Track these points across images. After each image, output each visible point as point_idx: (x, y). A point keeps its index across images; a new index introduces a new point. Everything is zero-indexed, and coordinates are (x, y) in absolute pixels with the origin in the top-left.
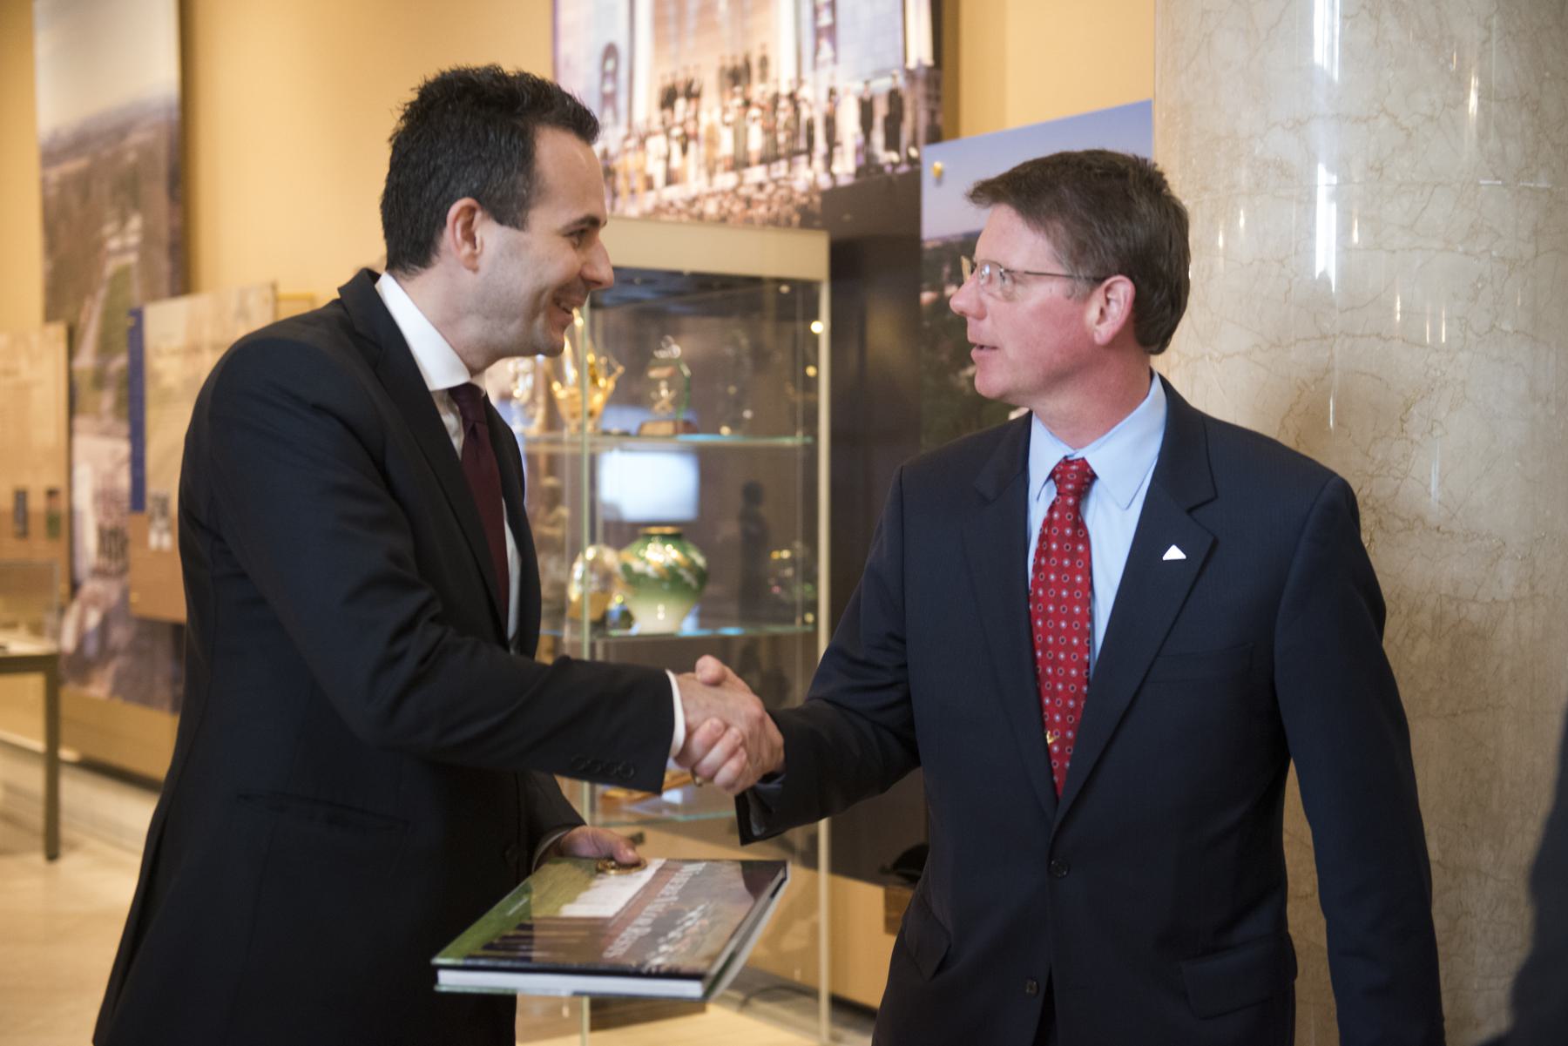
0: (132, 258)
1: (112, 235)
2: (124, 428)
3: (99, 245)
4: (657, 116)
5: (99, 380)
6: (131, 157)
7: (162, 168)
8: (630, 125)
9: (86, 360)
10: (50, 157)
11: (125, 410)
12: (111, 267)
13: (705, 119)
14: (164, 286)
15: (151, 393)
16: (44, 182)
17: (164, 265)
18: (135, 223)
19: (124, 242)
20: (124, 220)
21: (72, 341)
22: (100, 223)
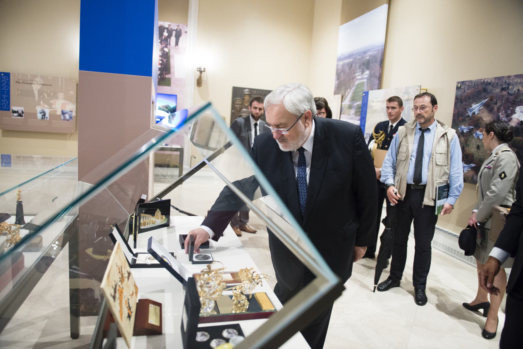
0: (366, 80)
1: (358, 76)
2: (359, 118)
3: (354, 78)
5: (350, 107)
6: (368, 58)
7: (379, 60)
9: (347, 102)
10: (340, 59)
11: (359, 114)
12: (357, 83)
14: (376, 87)
15: (369, 110)
16: (337, 65)
17: (377, 82)
18: (367, 72)
19: (362, 77)
20: (363, 72)
22: (355, 73)
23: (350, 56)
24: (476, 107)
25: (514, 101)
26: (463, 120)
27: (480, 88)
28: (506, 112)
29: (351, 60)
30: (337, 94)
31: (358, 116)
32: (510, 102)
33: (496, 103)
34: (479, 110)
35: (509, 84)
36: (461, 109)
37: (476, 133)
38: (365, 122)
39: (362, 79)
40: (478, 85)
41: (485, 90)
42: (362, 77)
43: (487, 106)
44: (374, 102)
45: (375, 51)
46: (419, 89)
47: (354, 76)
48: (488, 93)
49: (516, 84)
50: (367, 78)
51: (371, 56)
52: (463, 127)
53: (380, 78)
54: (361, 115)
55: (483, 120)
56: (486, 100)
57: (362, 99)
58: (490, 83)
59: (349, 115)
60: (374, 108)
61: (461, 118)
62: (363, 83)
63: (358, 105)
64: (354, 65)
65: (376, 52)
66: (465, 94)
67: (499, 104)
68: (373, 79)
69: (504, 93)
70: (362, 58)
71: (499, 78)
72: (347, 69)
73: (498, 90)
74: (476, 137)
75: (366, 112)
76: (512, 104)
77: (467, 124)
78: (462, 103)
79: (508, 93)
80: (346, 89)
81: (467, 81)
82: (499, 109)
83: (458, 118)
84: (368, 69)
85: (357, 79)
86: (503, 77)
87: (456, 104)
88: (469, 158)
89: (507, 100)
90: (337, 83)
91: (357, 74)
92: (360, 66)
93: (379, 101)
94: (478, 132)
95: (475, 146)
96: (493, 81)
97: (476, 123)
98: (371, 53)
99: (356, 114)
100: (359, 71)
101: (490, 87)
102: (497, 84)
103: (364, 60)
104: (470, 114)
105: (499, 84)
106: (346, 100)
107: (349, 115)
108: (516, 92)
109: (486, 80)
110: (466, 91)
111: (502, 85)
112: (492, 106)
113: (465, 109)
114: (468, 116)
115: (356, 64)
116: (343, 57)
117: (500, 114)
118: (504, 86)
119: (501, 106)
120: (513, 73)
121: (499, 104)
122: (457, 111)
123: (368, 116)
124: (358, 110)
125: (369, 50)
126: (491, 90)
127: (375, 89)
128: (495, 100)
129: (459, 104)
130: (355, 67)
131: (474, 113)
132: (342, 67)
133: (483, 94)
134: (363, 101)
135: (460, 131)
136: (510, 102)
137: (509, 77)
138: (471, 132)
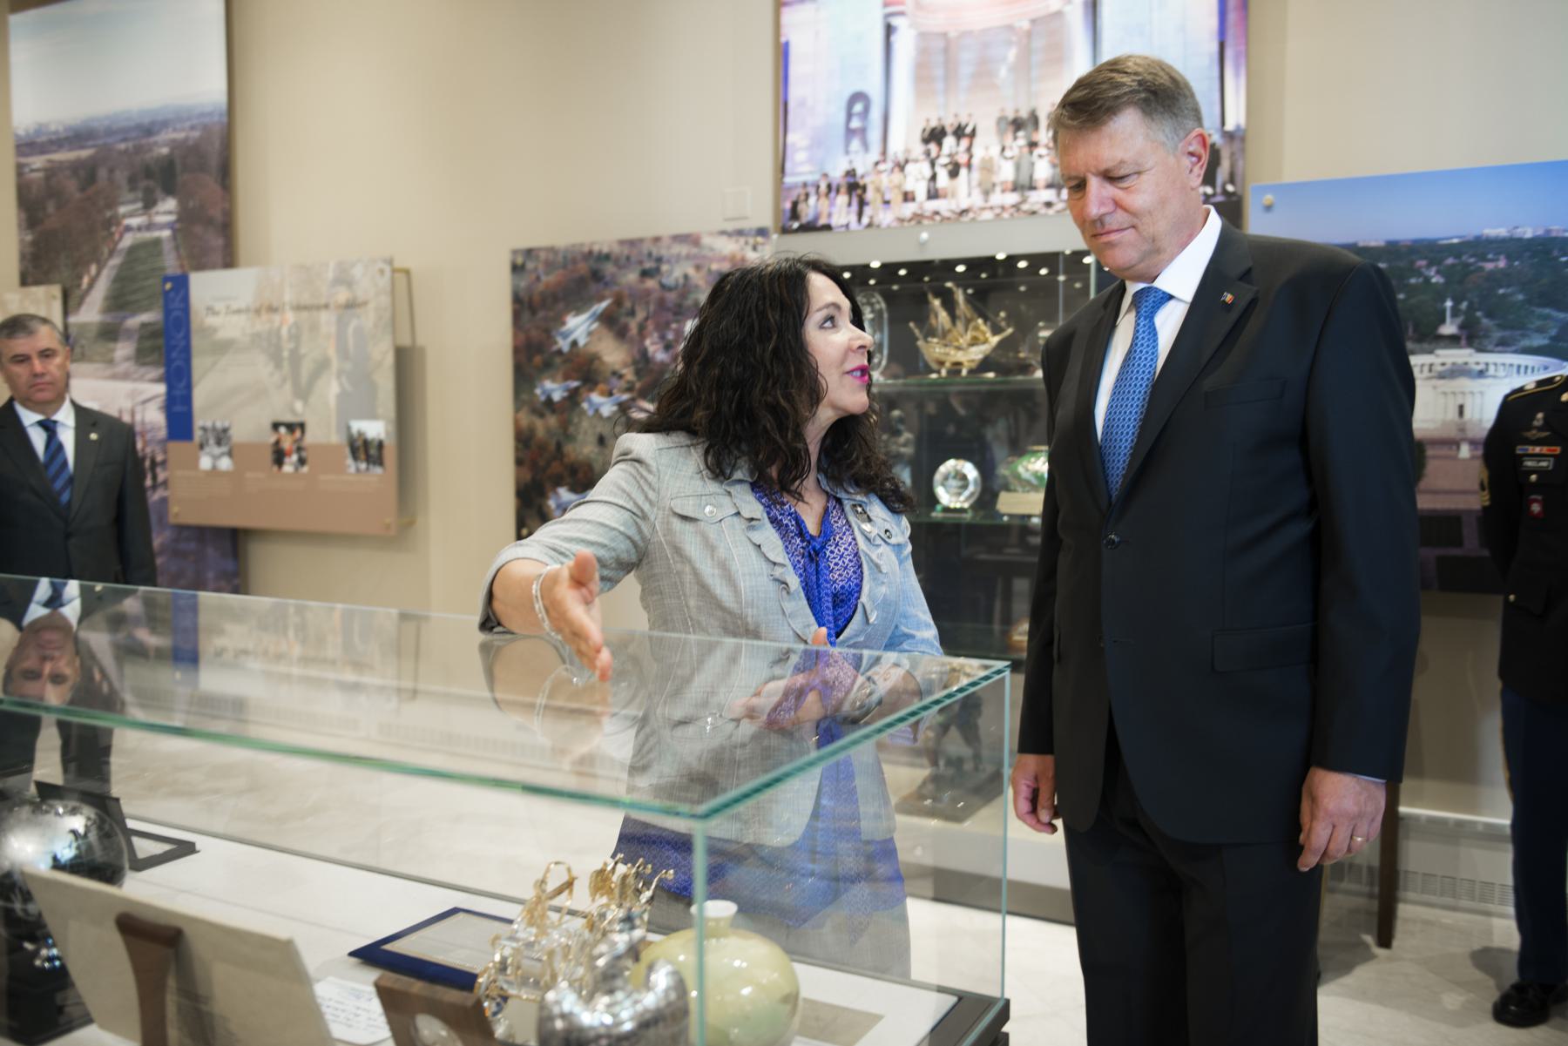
0: (166, 233)
1: (131, 215)
2: (159, 371)
3: (115, 220)
4: (918, 149)
5: (109, 333)
6: (165, 151)
7: (214, 162)
8: (884, 153)
9: (90, 313)
12: (127, 241)
13: (978, 153)
15: (196, 342)
16: (20, 168)
17: (218, 242)
18: (170, 204)
20: (149, 204)
21: (70, 302)
22: (112, 204)
23: (78, 136)
24: (578, 327)
25: (679, 306)
26: (547, 366)
27: (583, 268)
28: (662, 337)
29: (85, 153)
30: (37, 283)
31: (154, 364)
32: (668, 310)
33: (632, 313)
34: (590, 334)
35: (659, 260)
36: (534, 333)
37: (590, 402)
38: (189, 387)
39: (150, 227)
40: (574, 261)
41: (596, 276)
42: (150, 222)
43: (609, 320)
44: (215, 313)
45: (193, 128)
46: (387, 269)
47: (108, 214)
48: (606, 284)
49: (678, 258)
50: (170, 225)
51: (174, 144)
52: (548, 384)
53: (227, 228)
54: (168, 363)
55: (603, 363)
56: (604, 305)
57: (161, 302)
58: (607, 257)
59: (111, 362)
60: (222, 335)
61: (538, 359)
62: (157, 242)
63: (144, 325)
64: (102, 173)
65: (196, 134)
66: (541, 287)
67: (640, 315)
68: (198, 229)
69: (651, 283)
70: (139, 149)
71: (632, 243)
72: (71, 186)
73: (631, 277)
74: (591, 413)
75: (186, 352)
76: (676, 314)
77: (560, 376)
78: (533, 311)
79: (663, 287)
80: (79, 266)
81: (539, 249)
82: (642, 328)
83: (530, 359)
84: (170, 190)
85: (128, 229)
86: (641, 240)
87: (517, 316)
88: (580, 475)
89: (661, 303)
90: (29, 238)
91: (122, 210)
92: (133, 182)
93: (239, 311)
94: (596, 397)
95: (592, 439)
96: (616, 249)
97: (586, 371)
98: (180, 136)
99: (141, 357)
100: (131, 196)
101: (609, 269)
102: (628, 258)
103: (148, 156)
104: (564, 345)
105: (633, 259)
106: (84, 308)
107: (111, 362)
108: (681, 281)
109: (596, 248)
110: (544, 279)
111: (641, 262)
112: (623, 320)
113: (548, 334)
114: (560, 352)
115: (111, 171)
116: (44, 138)
117: (648, 342)
118: (648, 265)
119: (646, 319)
120: (666, 229)
121: (640, 315)
122: (522, 336)
123: (199, 364)
124: (148, 344)
125: (165, 124)
126: (613, 276)
127: (213, 267)
128: (628, 304)
129: (526, 316)
130: (111, 180)
131: (574, 343)
132: (47, 178)
133: (593, 287)
134: (167, 312)
135: (543, 398)
136: (668, 310)
137: (657, 240)
138: (573, 398)
